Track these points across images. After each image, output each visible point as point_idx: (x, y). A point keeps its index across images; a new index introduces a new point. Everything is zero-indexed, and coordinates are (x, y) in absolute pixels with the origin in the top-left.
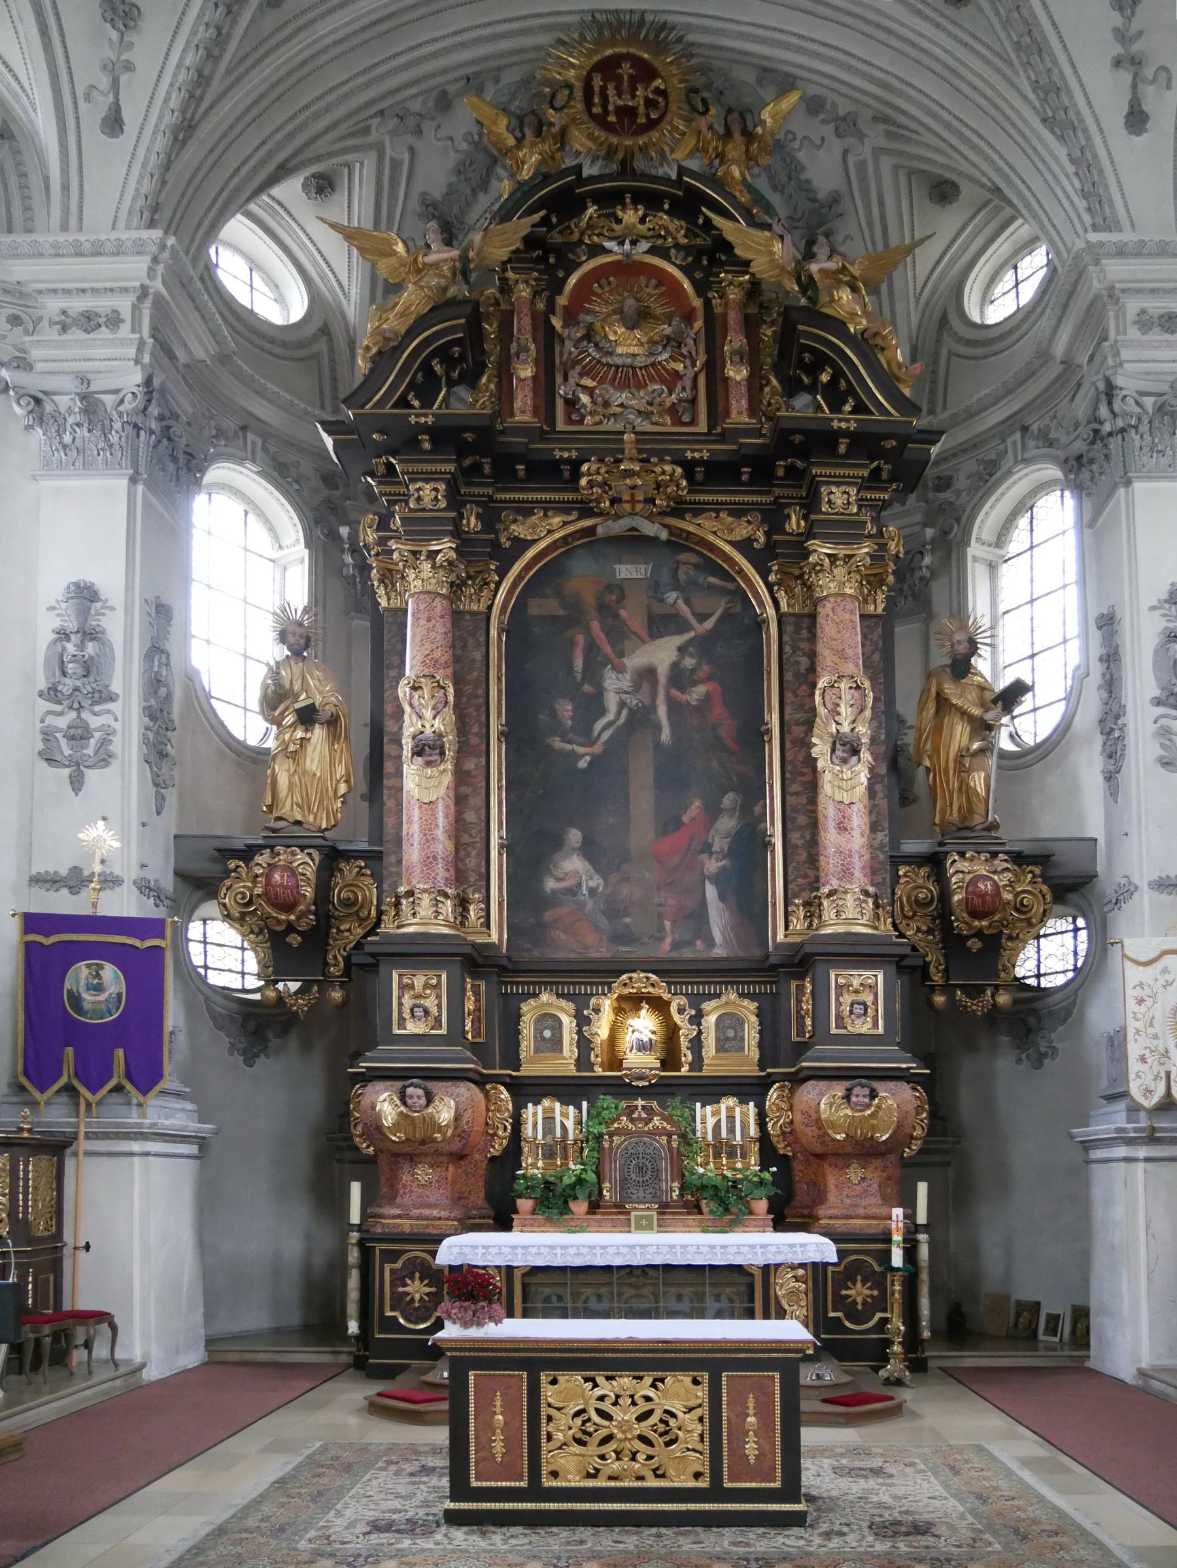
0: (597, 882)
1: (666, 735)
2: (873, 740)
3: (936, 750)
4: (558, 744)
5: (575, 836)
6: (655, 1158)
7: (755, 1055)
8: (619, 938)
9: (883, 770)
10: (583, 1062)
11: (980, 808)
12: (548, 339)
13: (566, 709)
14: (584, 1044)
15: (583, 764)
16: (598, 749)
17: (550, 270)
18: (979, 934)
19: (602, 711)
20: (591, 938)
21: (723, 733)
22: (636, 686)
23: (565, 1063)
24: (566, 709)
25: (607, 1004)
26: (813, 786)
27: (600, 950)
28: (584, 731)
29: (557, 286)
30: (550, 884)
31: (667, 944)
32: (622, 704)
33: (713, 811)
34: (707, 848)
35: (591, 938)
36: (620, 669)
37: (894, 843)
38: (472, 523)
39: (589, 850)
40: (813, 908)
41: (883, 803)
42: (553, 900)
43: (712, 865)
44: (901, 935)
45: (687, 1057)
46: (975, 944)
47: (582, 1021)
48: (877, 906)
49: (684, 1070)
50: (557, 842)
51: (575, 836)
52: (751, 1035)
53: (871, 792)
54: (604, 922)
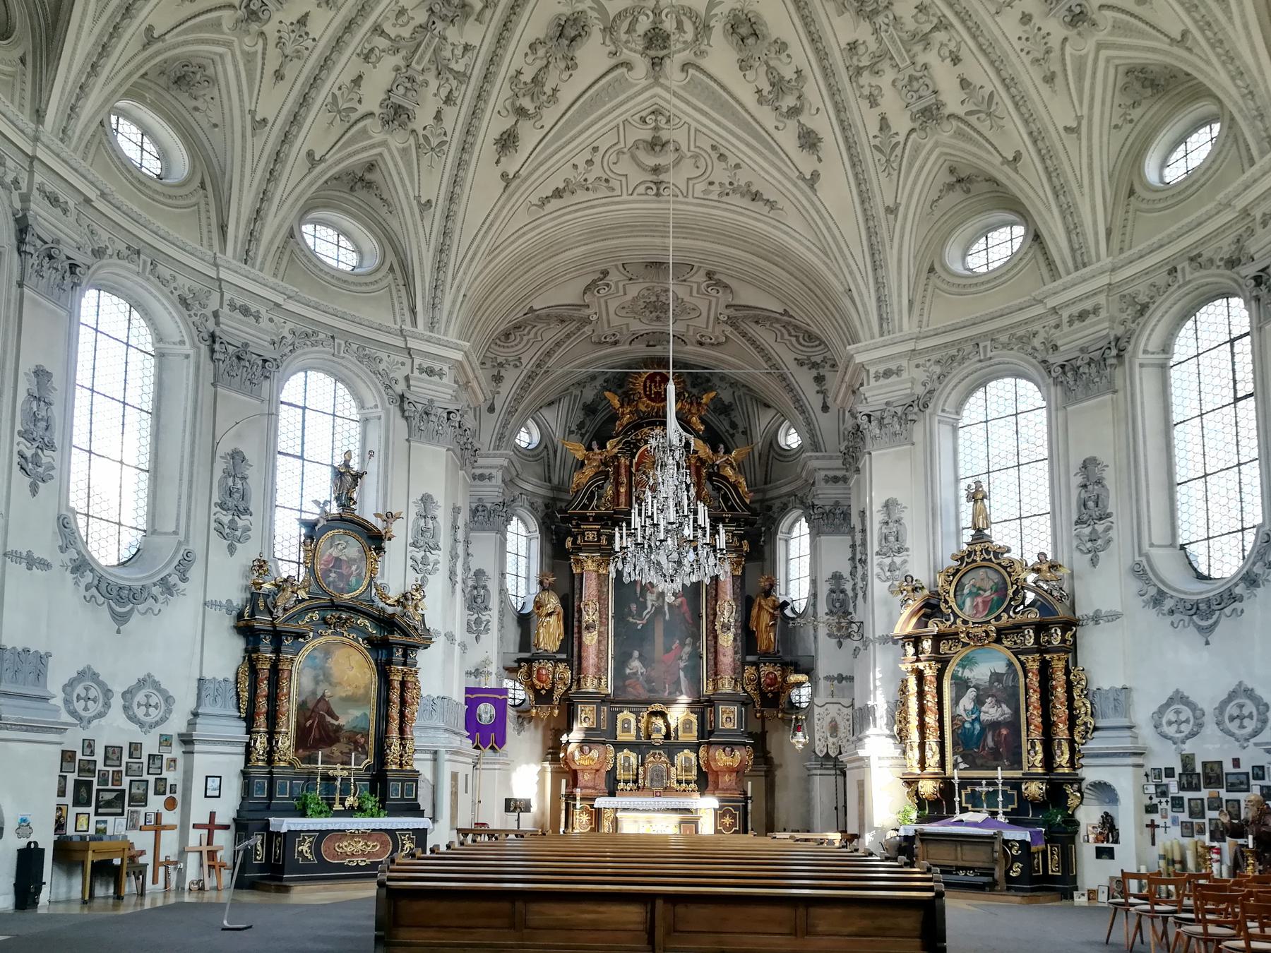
0: (643, 670)
1: (667, 617)
2: (736, 621)
3: (758, 623)
4: (631, 620)
5: (636, 654)
6: (662, 771)
7: (696, 734)
8: (651, 691)
9: (739, 631)
10: (638, 736)
11: (772, 646)
12: (630, 475)
13: (634, 607)
14: (638, 729)
15: (639, 627)
16: (644, 622)
17: (631, 450)
18: (771, 691)
19: (646, 608)
20: (641, 691)
21: (687, 615)
22: (658, 598)
23: (630, 737)
24: (634, 607)
25: (645, 715)
26: (716, 637)
27: (644, 695)
28: (640, 615)
29: (633, 456)
30: (628, 671)
31: (666, 694)
32: (653, 605)
33: (683, 645)
34: (681, 658)
35: (641, 691)
36: (652, 593)
37: (744, 658)
38: (604, 542)
39: (641, 658)
40: (715, 683)
41: (740, 644)
42: (629, 677)
43: (682, 665)
44: (745, 692)
45: (673, 735)
46: (770, 695)
47: (638, 721)
48: (736, 681)
49: (672, 740)
50: (630, 656)
51: (636, 654)
52: (695, 727)
53: (735, 640)
54: (646, 686)
